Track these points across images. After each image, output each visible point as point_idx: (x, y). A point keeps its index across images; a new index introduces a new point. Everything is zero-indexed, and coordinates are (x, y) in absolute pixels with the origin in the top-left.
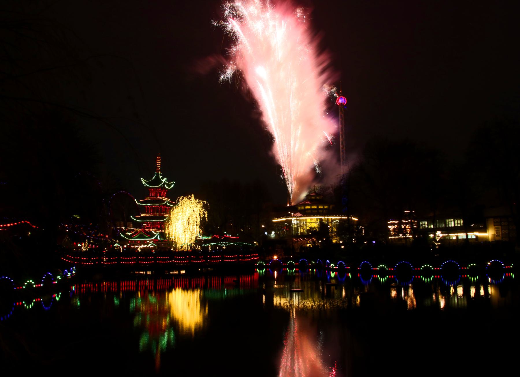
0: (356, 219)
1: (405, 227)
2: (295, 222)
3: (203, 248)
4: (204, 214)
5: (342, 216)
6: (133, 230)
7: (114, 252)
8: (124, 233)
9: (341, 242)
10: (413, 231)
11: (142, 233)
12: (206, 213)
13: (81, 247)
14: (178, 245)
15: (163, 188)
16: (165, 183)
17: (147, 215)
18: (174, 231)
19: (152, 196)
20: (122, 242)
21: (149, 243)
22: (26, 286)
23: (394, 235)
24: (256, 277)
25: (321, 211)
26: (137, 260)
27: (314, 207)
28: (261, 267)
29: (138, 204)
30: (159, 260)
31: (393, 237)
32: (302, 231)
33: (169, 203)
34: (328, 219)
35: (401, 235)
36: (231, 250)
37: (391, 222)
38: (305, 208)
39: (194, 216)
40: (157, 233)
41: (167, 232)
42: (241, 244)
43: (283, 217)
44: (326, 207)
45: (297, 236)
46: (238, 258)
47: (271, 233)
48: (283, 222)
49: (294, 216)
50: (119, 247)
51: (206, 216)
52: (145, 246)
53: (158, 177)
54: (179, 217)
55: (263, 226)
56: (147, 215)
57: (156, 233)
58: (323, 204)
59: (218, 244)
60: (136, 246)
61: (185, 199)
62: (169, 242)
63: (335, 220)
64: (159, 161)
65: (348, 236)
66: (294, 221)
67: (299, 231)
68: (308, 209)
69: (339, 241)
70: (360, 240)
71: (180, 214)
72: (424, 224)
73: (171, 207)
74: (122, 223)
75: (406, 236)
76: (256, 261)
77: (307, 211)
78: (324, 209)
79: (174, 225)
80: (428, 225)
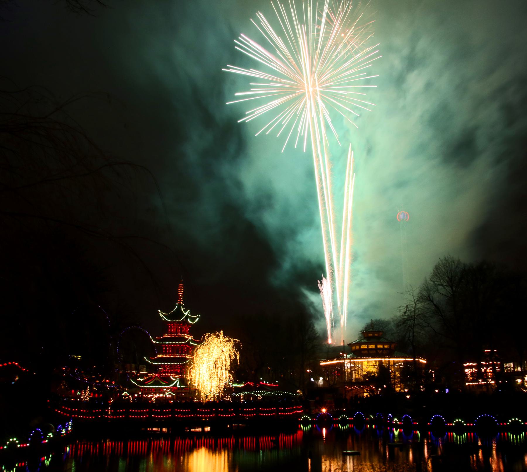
0: (425, 362)
1: (485, 370)
2: (349, 366)
3: (234, 398)
4: (236, 356)
5: (406, 358)
6: (146, 375)
7: (121, 403)
8: (135, 378)
9: (406, 390)
10: (496, 376)
11: (157, 379)
12: (238, 354)
13: (81, 395)
14: (202, 394)
15: (185, 322)
16: (187, 317)
17: (165, 356)
18: (197, 376)
19: (171, 333)
20: (132, 389)
21: (166, 391)
22: (9, 446)
23: (472, 381)
24: (299, 434)
25: (380, 352)
26: (150, 413)
27: (372, 346)
28: (306, 423)
29: (154, 342)
30: (178, 413)
31: (471, 384)
32: (357, 377)
33: (192, 341)
34: (389, 361)
35: (480, 380)
36: (267, 401)
37: (468, 364)
38: (360, 347)
39: (223, 358)
40: (176, 378)
41: (188, 378)
42: (281, 393)
43: (332, 359)
44: (386, 346)
45: (351, 383)
46: (278, 411)
47: (319, 379)
48: (333, 366)
49: (347, 359)
50: (128, 396)
51: (238, 358)
52: (161, 395)
53: (179, 309)
54: (204, 359)
55: (308, 371)
56: (165, 356)
57: (175, 379)
58: (383, 343)
59: (252, 393)
60: (150, 396)
61: (213, 336)
62: (190, 390)
63: (398, 362)
64: (181, 289)
65: (414, 383)
66: (347, 364)
67: (354, 376)
68: (364, 349)
69: (404, 389)
70: (430, 387)
71: (205, 355)
72: (510, 367)
73: (195, 347)
74: (133, 365)
75: (487, 381)
76: (300, 415)
77: (363, 352)
78: (383, 349)
79: (198, 370)
80: (514, 367)
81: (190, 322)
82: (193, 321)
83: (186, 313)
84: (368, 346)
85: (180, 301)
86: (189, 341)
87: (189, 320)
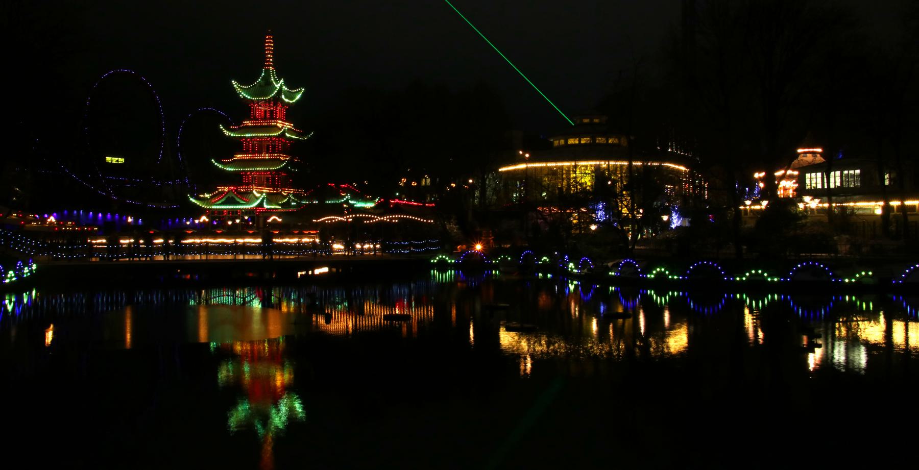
11: (230, 195)
15: (277, 99)
16: (280, 91)
29: (227, 133)
38: (566, 142)
64: (269, 45)
81: (287, 100)
82: (292, 99)
83: (278, 86)
84: (580, 141)
85: (269, 65)
86: (284, 131)
87: (283, 97)
